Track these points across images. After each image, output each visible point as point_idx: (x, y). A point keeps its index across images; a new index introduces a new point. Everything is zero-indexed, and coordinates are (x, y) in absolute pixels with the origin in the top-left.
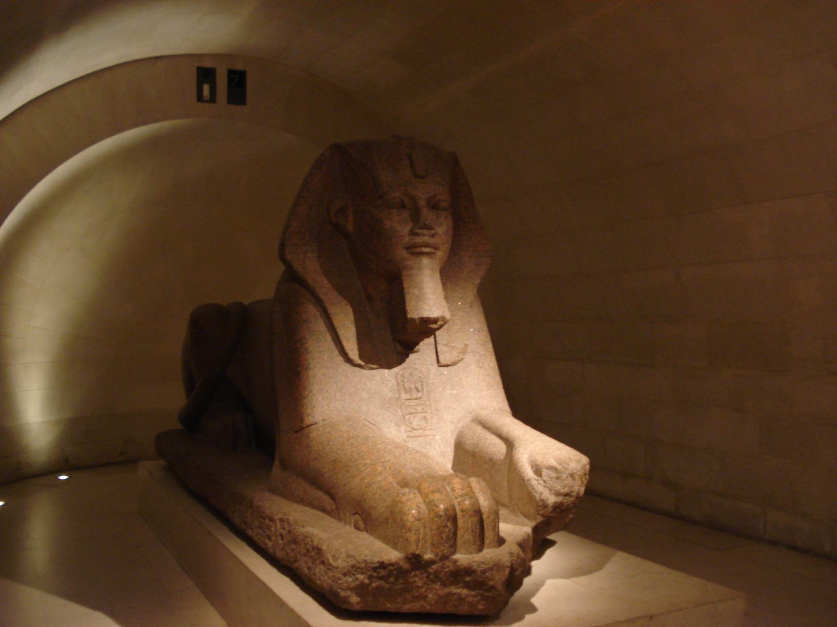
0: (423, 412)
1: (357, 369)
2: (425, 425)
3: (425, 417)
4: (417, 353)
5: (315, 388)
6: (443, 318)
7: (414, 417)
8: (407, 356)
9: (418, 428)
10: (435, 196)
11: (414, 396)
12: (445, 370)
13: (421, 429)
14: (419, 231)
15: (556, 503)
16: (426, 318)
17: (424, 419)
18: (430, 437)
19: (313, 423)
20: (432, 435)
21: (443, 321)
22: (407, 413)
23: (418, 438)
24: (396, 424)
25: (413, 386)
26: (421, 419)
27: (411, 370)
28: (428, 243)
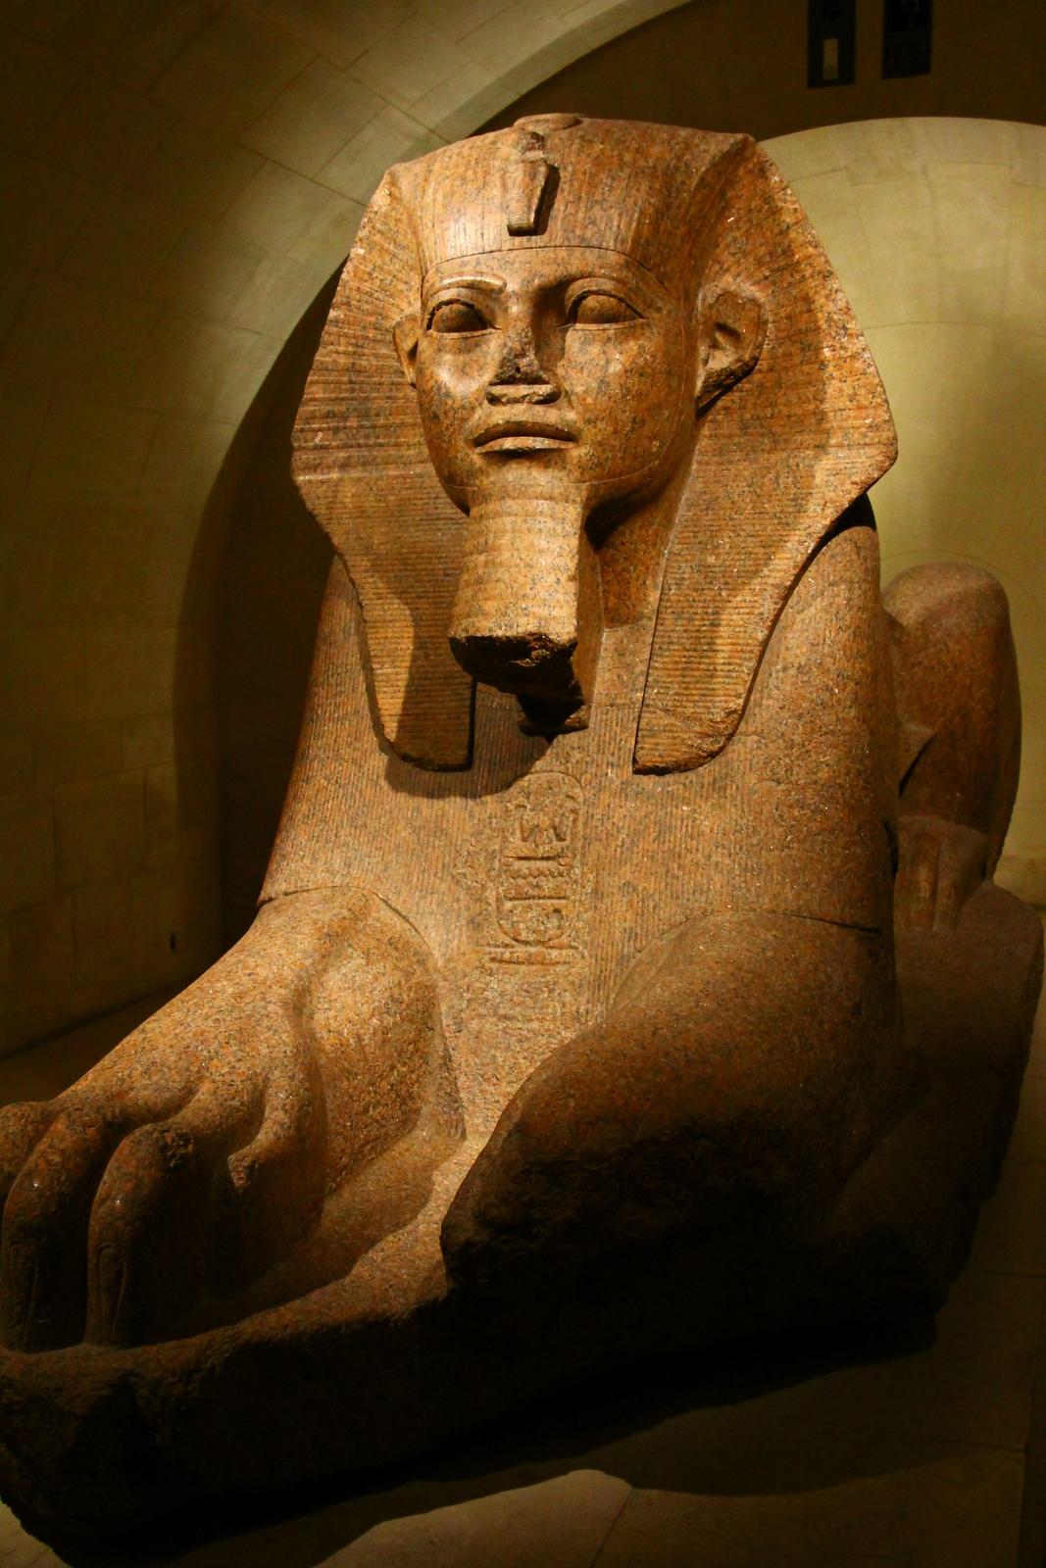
0: (559, 898)
3: (557, 911)
4: (581, 733)
5: (303, 808)
6: (540, 638)
7: (530, 907)
8: (550, 741)
9: (531, 939)
10: (563, 284)
11: (540, 852)
12: (649, 782)
13: (539, 943)
14: (498, 390)
15: (468, 1244)
16: (483, 638)
17: (555, 921)
19: (267, 899)
20: (565, 963)
21: (544, 647)
23: (523, 968)
24: (472, 921)
25: (544, 820)
26: (547, 916)
27: (555, 775)
28: (519, 424)
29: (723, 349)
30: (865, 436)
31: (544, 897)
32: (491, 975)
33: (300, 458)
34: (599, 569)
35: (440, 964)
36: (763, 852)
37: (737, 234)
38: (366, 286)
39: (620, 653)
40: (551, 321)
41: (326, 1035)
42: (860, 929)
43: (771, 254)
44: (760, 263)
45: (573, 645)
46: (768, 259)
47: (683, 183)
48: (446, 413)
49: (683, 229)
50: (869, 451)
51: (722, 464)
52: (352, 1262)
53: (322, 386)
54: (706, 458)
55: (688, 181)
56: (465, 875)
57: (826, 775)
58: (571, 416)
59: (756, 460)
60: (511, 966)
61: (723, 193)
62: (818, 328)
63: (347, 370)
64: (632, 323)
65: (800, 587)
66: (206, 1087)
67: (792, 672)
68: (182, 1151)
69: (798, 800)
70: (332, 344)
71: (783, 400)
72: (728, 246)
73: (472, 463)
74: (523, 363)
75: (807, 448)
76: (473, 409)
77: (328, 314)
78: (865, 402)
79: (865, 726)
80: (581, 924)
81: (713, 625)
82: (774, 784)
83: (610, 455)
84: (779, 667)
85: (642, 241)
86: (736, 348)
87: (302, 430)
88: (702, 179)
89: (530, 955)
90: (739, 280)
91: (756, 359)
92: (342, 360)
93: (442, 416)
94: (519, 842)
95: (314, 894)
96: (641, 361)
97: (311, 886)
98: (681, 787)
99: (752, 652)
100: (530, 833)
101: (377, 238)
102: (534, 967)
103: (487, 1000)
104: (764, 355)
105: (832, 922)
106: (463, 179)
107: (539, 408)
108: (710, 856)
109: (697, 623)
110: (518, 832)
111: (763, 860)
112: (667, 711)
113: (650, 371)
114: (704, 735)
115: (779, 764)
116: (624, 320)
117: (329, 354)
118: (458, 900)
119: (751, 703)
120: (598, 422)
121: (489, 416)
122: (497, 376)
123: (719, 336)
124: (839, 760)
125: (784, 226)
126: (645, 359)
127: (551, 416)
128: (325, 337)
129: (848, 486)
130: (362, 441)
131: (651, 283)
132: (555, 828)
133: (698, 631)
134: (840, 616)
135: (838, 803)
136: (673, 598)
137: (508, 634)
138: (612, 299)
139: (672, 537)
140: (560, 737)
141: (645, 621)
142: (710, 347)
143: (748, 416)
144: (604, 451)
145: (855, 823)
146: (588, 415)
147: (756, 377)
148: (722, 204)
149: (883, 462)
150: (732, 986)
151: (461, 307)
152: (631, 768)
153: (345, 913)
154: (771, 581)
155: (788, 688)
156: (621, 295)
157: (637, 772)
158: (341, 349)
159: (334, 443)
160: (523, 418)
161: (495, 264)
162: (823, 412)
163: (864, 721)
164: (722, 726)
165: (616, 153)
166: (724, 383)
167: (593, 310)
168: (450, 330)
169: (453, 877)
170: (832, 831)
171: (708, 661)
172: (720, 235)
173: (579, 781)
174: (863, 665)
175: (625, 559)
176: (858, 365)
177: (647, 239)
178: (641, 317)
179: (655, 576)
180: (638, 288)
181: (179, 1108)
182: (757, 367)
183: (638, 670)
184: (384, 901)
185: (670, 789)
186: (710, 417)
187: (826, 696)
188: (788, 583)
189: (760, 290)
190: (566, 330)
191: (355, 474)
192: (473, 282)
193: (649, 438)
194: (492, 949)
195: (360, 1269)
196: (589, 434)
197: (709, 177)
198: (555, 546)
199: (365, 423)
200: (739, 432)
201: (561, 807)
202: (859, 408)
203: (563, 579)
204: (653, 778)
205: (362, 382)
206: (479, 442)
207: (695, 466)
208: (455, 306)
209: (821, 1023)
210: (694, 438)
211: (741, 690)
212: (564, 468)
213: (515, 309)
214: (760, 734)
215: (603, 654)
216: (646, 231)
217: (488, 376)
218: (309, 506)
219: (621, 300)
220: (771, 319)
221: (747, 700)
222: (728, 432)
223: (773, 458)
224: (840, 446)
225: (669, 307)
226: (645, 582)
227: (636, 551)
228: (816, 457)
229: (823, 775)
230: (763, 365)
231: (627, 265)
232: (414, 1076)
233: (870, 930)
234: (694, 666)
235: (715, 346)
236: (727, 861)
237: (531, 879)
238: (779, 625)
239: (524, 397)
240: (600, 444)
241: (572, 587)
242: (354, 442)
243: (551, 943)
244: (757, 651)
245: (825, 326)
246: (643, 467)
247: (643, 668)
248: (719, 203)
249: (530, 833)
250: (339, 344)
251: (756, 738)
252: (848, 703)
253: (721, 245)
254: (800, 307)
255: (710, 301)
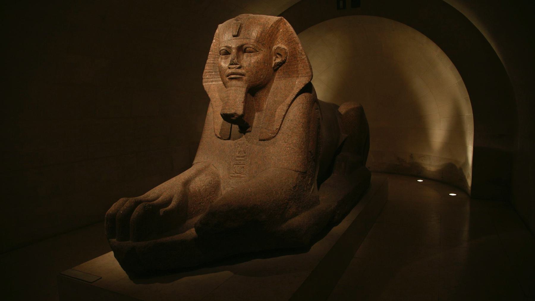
0: (244, 165)
1: (219, 139)
2: (242, 171)
3: (243, 167)
4: (250, 133)
6: (235, 113)
8: (244, 134)
9: (238, 172)
10: (242, 46)
11: (242, 155)
12: (262, 142)
13: (240, 173)
14: (230, 66)
18: (243, 178)
22: (236, 164)
23: (236, 178)
29: (279, 58)
30: (305, 75)
31: (241, 165)
32: (231, 179)
33: (204, 80)
34: (254, 101)
35: (222, 177)
36: (282, 156)
37: (282, 36)
38: (215, 48)
39: (258, 117)
40: (241, 53)
41: (191, 189)
42: (300, 172)
43: (288, 40)
44: (286, 42)
45: (243, 116)
46: (287, 40)
47: (267, 26)
48: (222, 71)
49: (268, 35)
50: (306, 78)
51: (279, 80)
52: (186, 230)
53: (208, 67)
54: (277, 79)
55: (268, 26)
56: (227, 160)
57: (295, 142)
58: (243, 71)
59: (286, 80)
60: (234, 178)
61: (277, 28)
62: (297, 54)
63: (212, 63)
64: (256, 53)
65: (293, 105)
66: (162, 197)
67: (290, 121)
68: (149, 208)
69: (289, 147)
70: (210, 58)
71: (291, 68)
72: (280, 38)
73: (226, 80)
74: (234, 61)
75: (295, 77)
76: (226, 70)
77: (209, 53)
78: (305, 68)
79: (304, 132)
80: (247, 170)
81: (275, 112)
82: (285, 143)
83: (251, 78)
84: (287, 120)
85: (258, 37)
86: (281, 57)
87: (204, 75)
88: (272, 25)
89: (238, 175)
90: (282, 45)
91: (286, 60)
92: (212, 62)
93: (221, 71)
94: (237, 154)
95: (201, 163)
96: (257, 60)
97: (200, 162)
98: (267, 144)
99: (281, 117)
100: (239, 152)
101: (217, 38)
102: (239, 178)
103: (229, 184)
104: (287, 59)
105: (293, 170)
106: (227, 27)
107: (237, 70)
108: (272, 157)
109: (272, 111)
110: (238, 153)
111: (281, 158)
112: (265, 128)
113: (259, 62)
114: (271, 133)
115: (286, 139)
116: (254, 52)
117: (209, 61)
118: (226, 165)
119: (281, 127)
120: (249, 72)
121: (229, 71)
122: (230, 63)
123: (278, 56)
124: (298, 138)
125: (290, 34)
126: (259, 60)
127: (240, 71)
128: (208, 57)
129: (302, 84)
130: (215, 77)
131: (260, 45)
132: (244, 151)
133: (272, 113)
134: (300, 110)
135: (297, 147)
136: (269, 107)
137: (230, 113)
138: (252, 49)
139: (269, 95)
140: (246, 134)
141: (263, 111)
142: (276, 58)
143: (285, 71)
144: (250, 77)
145: (300, 151)
146: (247, 71)
147: (286, 63)
148: (278, 30)
149: (309, 80)
150: (264, 181)
151: (225, 51)
152: (258, 140)
153: (204, 167)
154: (286, 103)
155: (289, 124)
156: (254, 48)
157: (259, 140)
158: (211, 59)
159: (210, 77)
160: (234, 71)
161: (230, 42)
162: (298, 70)
163: (304, 131)
164: (275, 132)
165: (254, 21)
166: (280, 65)
167: (248, 51)
168: (223, 55)
169: (225, 160)
170: (295, 152)
171: (273, 119)
172: (278, 36)
173: (249, 142)
174: (305, 120)
175: (259, 99)
176: (304, 61)
177: (259, 37)
178: (258, 52)
179: (265, 102)
180: (257, 46)
181: (155, 200)
182: (286, 62)
183: (261, 121)
184: (213, 165)
185: (265, 144)
186: (278, 71)
187: (296, 126)
188: (289, 104)
189: (286, 47)
190: (244, 55)
191: (214, 83)
192: (227, 46)
193: (260, 75)
194: (231, 174)
195: (187, 232)
196: (247, 74)
197: (273, 25)
198: (240, 96)
199: (216, 73)
200: (282, 74)
201: (245, 147)
202: (304, 69)
203: (241, 102)
204: (263, 141)
205: (215, 66)
206: (228, 76)
207: (275, 81)
208: (223, 51)
209: (282, 190)
210: (274, 75)
211: (279, 125)
212: (242, 81)
213: (234, 51)
214: (283, 133)
215: (255, 117)
216: (259, 35)
217: (229, 64)
218: (205, 89)
219: (253, 49)
220: (288, 52)
221: (280, 126)
222: (281, 74)
223: (289, 79)
224: (301, 77)
225: (265, 50)
226: (263, 104)
227: (261, 97)
228: (297, 79)
229: (294, 141)
230: (287, 61)
231: (255, 42)
232: (214, 198)
233: (302, 172)
234: (271, 120)
235: (277, 57)
236: (275, 158)
237: (239, 161)
238: (288, 112)
239: (234, 67)
240: (249, 76)
241: (242, 104)
242: (214, 77)
243: (242, 173)
244: (283, 117)
245: (298, 53)
246: (259, 81)
247: (262, 120)
248: (277, 30)
249: (239, 152)
250: (211, 59)
251: (282, 134)
252: (301, 127)
253: (278, 38)
254: (294, 50)
255: (275, 49)
